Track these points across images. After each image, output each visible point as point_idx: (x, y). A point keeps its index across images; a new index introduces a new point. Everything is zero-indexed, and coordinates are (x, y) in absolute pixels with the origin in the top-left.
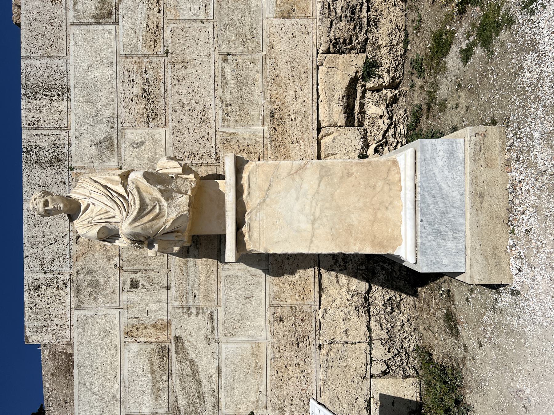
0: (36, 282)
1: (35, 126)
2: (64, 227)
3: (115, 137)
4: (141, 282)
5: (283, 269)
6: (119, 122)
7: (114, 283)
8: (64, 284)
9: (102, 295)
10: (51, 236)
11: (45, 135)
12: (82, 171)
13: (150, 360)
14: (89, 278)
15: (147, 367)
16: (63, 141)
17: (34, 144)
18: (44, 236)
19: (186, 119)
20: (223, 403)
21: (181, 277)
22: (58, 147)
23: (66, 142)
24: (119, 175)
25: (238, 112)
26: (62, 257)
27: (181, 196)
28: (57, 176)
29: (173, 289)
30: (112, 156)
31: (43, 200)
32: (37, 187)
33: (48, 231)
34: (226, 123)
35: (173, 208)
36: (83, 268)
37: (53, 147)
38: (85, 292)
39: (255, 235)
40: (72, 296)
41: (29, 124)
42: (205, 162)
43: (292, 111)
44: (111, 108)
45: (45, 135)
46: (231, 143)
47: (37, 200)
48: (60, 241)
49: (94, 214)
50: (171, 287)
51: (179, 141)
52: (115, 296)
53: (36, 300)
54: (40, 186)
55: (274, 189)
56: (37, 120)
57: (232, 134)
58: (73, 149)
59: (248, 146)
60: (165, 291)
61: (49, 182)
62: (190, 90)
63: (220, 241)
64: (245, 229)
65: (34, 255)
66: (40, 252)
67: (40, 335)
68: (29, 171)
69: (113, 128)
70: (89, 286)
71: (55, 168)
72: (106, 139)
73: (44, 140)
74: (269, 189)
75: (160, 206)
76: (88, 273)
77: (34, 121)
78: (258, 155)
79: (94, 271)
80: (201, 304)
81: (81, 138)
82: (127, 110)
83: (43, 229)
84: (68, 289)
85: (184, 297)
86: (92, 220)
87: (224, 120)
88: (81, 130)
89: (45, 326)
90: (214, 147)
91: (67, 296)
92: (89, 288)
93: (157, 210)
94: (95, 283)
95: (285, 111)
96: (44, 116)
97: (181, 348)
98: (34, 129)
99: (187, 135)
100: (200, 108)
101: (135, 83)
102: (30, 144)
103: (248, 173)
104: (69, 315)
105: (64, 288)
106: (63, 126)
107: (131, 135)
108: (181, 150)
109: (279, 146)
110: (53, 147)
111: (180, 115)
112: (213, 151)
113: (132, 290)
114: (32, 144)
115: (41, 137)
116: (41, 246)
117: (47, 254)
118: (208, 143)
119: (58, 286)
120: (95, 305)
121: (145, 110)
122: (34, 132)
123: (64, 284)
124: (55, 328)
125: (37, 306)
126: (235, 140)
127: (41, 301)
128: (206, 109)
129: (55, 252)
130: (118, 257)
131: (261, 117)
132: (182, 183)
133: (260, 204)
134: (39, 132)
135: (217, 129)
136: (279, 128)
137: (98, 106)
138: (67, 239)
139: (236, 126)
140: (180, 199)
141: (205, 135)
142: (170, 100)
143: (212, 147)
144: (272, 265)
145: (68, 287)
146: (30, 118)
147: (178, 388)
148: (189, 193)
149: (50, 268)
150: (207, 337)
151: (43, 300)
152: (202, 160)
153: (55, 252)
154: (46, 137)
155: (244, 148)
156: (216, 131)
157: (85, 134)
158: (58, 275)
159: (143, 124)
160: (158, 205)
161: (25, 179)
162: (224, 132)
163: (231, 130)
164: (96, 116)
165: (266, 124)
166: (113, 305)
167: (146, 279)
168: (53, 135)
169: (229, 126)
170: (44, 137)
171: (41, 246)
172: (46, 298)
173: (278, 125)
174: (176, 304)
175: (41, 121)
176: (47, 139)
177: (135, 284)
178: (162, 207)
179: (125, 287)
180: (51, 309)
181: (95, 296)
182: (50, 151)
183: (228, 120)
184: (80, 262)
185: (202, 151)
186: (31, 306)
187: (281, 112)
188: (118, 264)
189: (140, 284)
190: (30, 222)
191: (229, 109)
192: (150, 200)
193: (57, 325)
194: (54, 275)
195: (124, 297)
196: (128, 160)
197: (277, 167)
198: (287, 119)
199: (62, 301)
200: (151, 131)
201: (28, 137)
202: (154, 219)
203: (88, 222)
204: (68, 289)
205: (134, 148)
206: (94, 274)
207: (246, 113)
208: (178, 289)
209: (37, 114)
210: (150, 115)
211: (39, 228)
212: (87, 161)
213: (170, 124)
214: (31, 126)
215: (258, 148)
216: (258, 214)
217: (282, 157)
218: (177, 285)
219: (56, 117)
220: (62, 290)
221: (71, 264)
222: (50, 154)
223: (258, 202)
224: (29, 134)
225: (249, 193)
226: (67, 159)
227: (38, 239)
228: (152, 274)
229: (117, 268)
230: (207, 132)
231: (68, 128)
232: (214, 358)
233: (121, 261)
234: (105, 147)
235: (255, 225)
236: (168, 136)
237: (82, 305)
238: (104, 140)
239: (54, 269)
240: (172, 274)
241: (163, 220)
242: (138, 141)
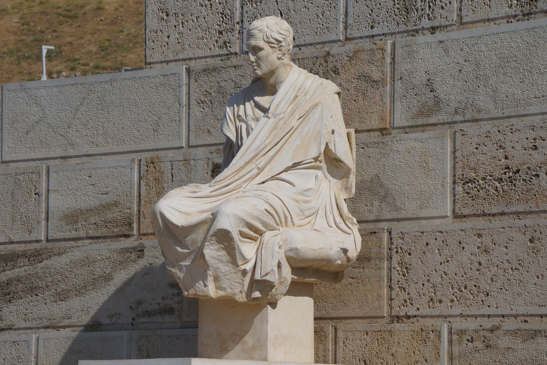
8: (225, 43)
13: (116, 204)
15: (106, 199)
20: (52, 333)
22: (430, 7)
23: (436, 23)
28: (383, 12)
62: (515, 265)
67: (155, 8)
69: (456, 112)
72: (438, 101)
87: (462, 332)
89: (167, 15)
97: (128, 258)
100: (485, 286)
101: (531, 152)
104: (181, 56)
111: (472, 244)
112: (412, 311)
113: (211, 167)
121: (482, 174)
124: (166, 34)
142: (498, 223)
147: (77, 254)
148: (221, 293)
150: (140, 303)
169: (450, 342)
185: (412, 289)
191: (479, 344)
193: (169, 37)
194: (238, 23)
226: (409, 28)
232: (112, 316)
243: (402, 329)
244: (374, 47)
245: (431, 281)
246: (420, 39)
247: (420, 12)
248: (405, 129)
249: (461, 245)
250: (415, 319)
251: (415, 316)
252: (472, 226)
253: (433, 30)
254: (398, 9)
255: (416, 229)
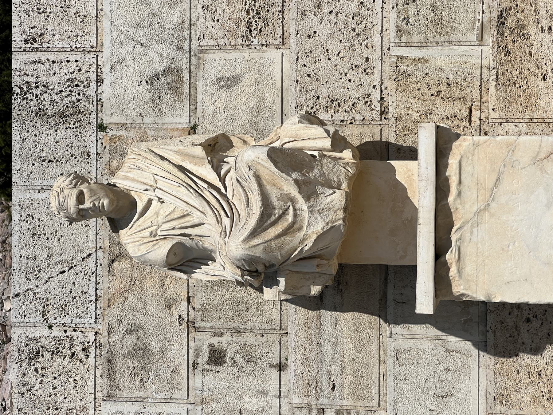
0: (33, 344)
1: (36, 45)
2: (86, 240)
3: (185, 66)
4: (230, 353)
5: (516, 341)
6: (193, 36)
7: (179, 352)
8: (84, 350)
9: (156, 375)
10: (63, 258)
11: (54, 62)
12: (122, 132)
14: (130, 340)
16: (87, 75)
17: (35, 80)
18: (49, 257)
19: (324, 30)
21: (308, 346)
22: (77, 86)
23: (93, 77)
24: (200, 145)
25: (430, 16)
26: (82, 299)
27: (331, 191)
28: (76, 142)
29: (291, 370)
30: (178, 104)
31: (75, 192)
32: (38, 162)
33: (56, 248)
34: (404, 39)
35: (317, 215)
36: (120, 322)
37: (69, 86)
38: (124, 367)
39: (469, 268)
40: (98, 375)
41: (26, 41)
42: (358, 117)
43: (543, 12)
44: (178, 9)
45: (54, 62)
46: (413, 79)
47: (66, 192)
48: (79, 268)
49: (160, 219)
50: (286, 366)
51: (309, 75)
52: (178, 377)
53: (32, 378)
54: (44, 161)
55: (506, 185)
56: (39, 32)
57: (415, 60)
58: (105, 87)
59: (448, 84)
60: (275, 373)
61: (61, 153)
63: (386, 279)
64: (450, 256)
65: (31, 293)
66: (42, 288)
68: (24, 132)
69: (181, 48)
70: (130, 355)
71: (72, 126)
72: (168, 71)
73: (52, 73)
74: (495, 186)
75: (295, 210)
76: (130, 331)
77: (34, 35)
78: (469, 103)
79: (141, 328)
80: (345, 403)
81: (120, 69)
82: (209, 14)
83: (48, 244)
84: (91, 359)
85: (311, 386)
86: (156, 230)
87: (400, 32)
88: (122, 53)
90: (378, 87)
91: (91, 375)
92: (129, 361)
93: (290, 218)
94: (141, 352)
95: (529, 12)
96: (53, 26)
98: (33, 50)
99: (324, 62)
102: (26, 79)
103: (458, 158)
105: (84, 358)
106: (87, 45)
107: (217, 63)
108: (313, 93)
109: (515, 84)
110: (69, 86)
111: (312, 23)
112: (376, 95)
114: (30, 79)
115: (47, 65)
116: (44, 275)
117: (54, 291)
118: (365, 79)
119: (73, 354)
120: (141, 394)
121: (244, 14)
122: (34, 56)
123: (84, 350)
125: (34, 390)
126: (422, 73)
127: (41, 382)
128: (364, 11)
129: (69, 287)
130: (186, 303)
131: (478, 25)
132: (331, 166)
133: (479, 212)
134: (43, 56)
135: (385, 50)
136: (515, 49)
137: (155, 7)
138: (91, 262)
139: (424, 44)
140: (329, 199)
141: (361, 62)
143: (374, 87)
144: (494, 332)
145: (92, 356)
146: (27, 28)
148: (344, 186)
149: (59, 319)
151: (45, 379)
152: (353, 114)
153: (69, 287)
154: (56, 67)
155: (439, 88)
156: (383, 54)
157: (129, 62)
158: (74, 333)
159: (240, 41)
160: (291, 208)
161: (16, 146)
162: (398, 57)
163: (414, 53)
164: (150, 25)
165: (487, 38)
166: (174, 396)
167: (238, 348)
168: (68, 61)
169: (409, 45)
170: (53, 66)
171: (44, 275)
172: (50, 376)
173: (514, 41)
174: (297, 400)
175: (48, 36)
176: (58, 70)
177: (217, 357)
178: (298, 212)
179: (199, 361)
180: (60, 398)
181: (140, 375)
182: (64, 94)
183: (409, 33)
184: (114, 308)
185: (354, 94)
186: (24, 389)
187: (520, 15)
188: (185, 316)
189: (227, 357)
190: (24, 230)
192: (279, 199)
194: (65, 331)
195: (197, 381)
196: (209, 111)
197: (511, 148)
198: (532, 30)
199: (80, 383)
200: (255, 55)
201: (23, 66)
202: (285, 233)
203: (151, 234)
204: (91, 359)
205: (221, 88)
206: (140, 334)
207: (446, 18)
208: (301, 371)
209: (39, 21)
210: (254, 23)
211: (40, 241)
212: (131, 113)
213: (292, 41)
214: (29, 45)
215: (469, 90)
216: (475, 230)
217: (520, 108)
218: (299, 363)
219: (75, 27)
220: (81, 361)
221: (99, 312)
222: (62, 99)
223: (475, 209)
224: (25, 59)
225: (459, 194)
226: (94, 109)
227: (38, 262)
228: (251, 339)
229: (185, 324)
230: (365, 56)
231: (97, 48)
233: (191, 310)
234: (165, 87)
235: (468, 250)
236: (286, 65)
237: (118, 393)
238: (164, 73)
239: (67, 320)
240: (290, 341)
241: (300, 235)
242: (229, 74)
243: (394, 104)
244: (108, 148)
245: (346, 71)
246: (105, 97)
247: (81, 97)
248: (193, 111)
249: (312, 34)
250: (385, 92)
251: (382, 91)
252: (294, 22)
253: (100, 81)
254: (74, 124)
255: (293, 90)
